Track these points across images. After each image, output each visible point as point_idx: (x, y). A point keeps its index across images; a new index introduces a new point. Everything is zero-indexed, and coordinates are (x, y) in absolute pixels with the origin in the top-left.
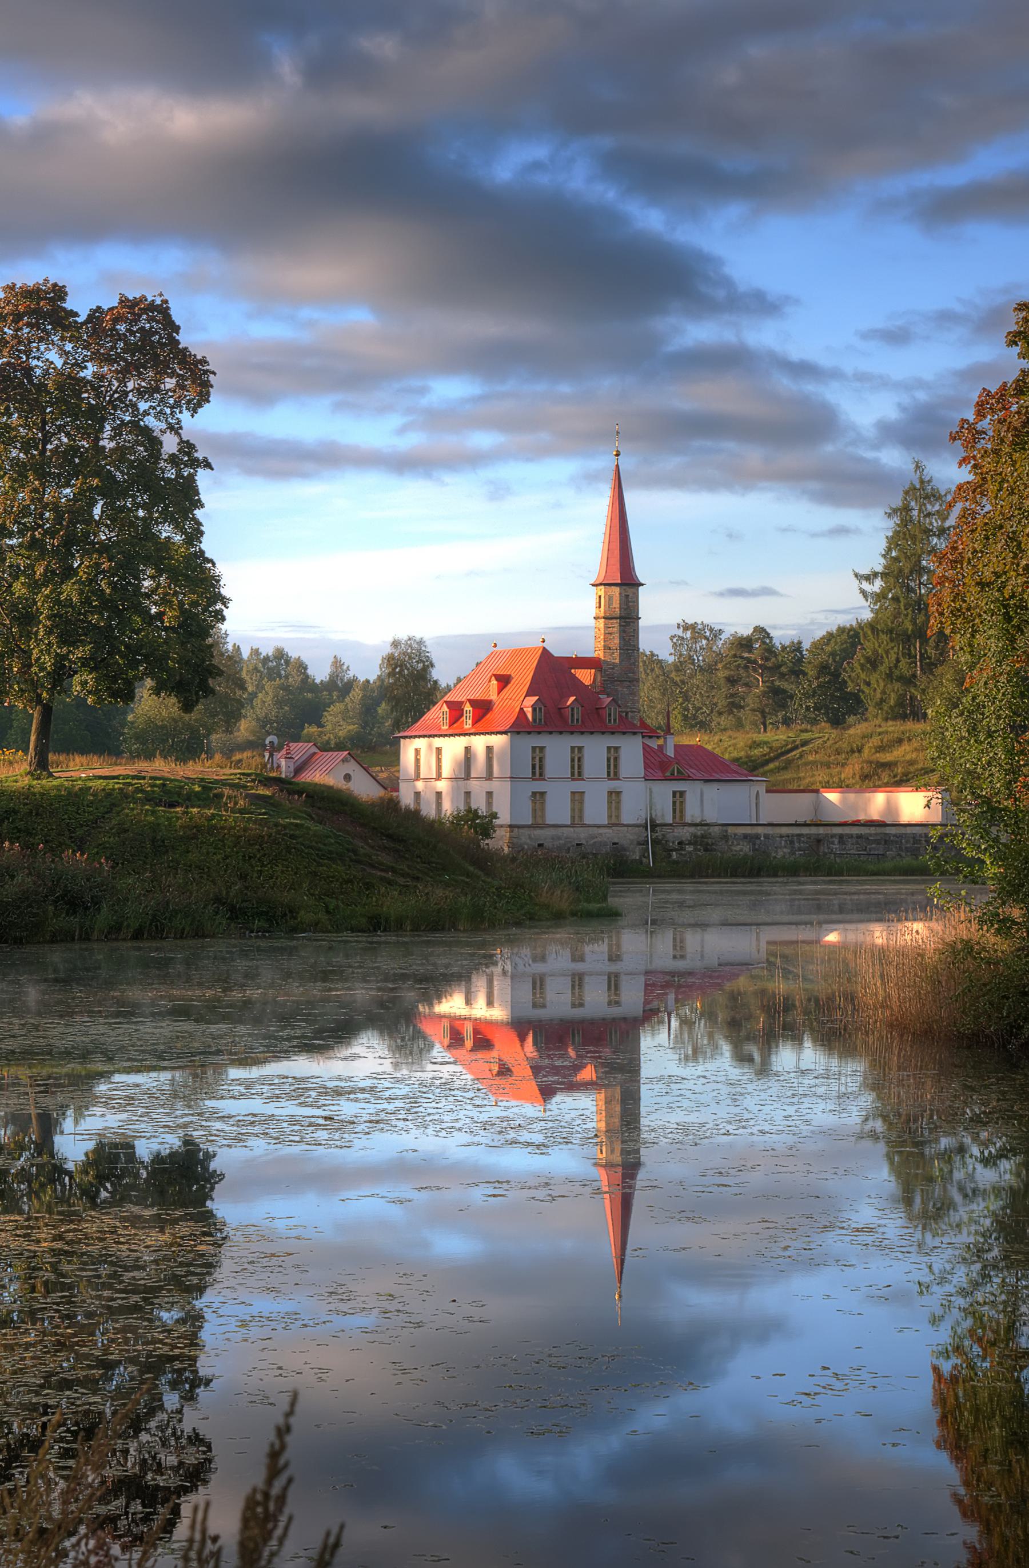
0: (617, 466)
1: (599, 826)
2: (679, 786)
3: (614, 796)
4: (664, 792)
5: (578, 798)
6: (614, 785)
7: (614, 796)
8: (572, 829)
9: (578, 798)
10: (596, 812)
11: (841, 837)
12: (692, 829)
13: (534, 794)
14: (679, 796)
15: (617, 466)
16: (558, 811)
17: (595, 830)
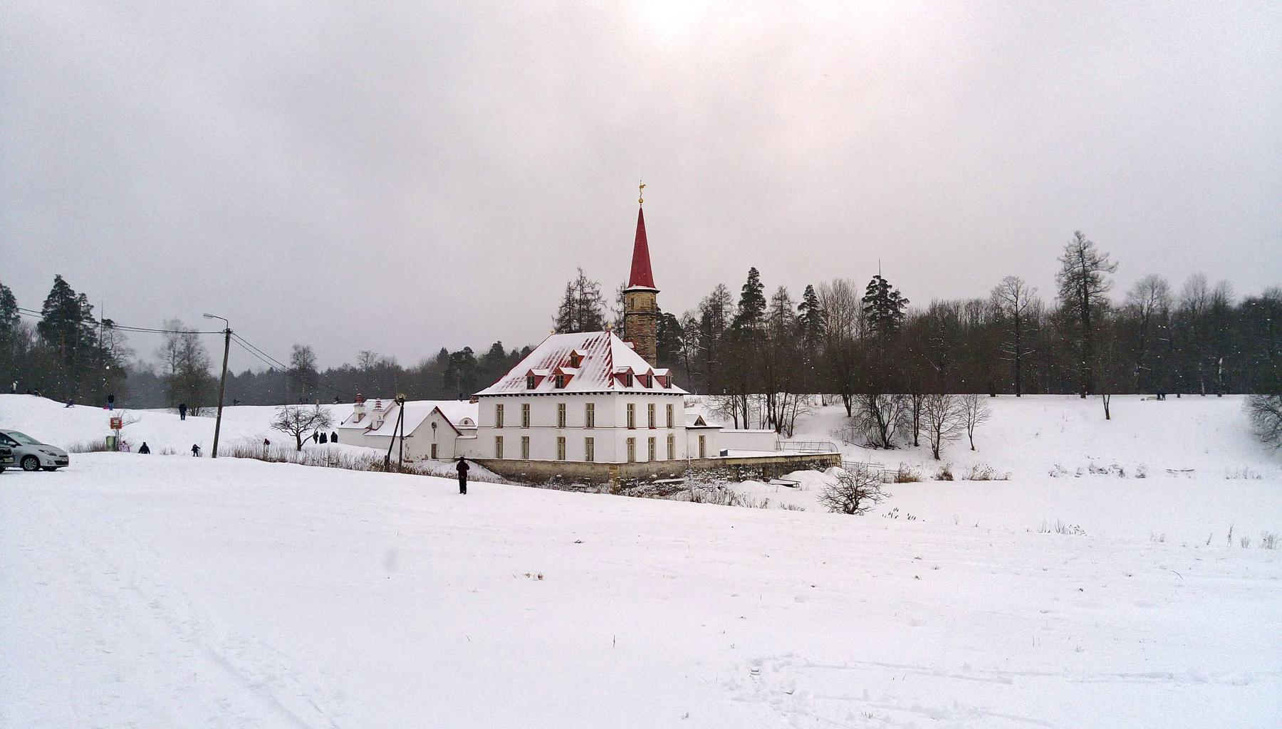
0: (641, 209)
1: (662, 462)
2: (703, 433)
3: (670, 439)
4: (694, 437)
5: (652, 440)
6: (671, 431)
7: (670, 439)
8: (647, 465)
9: (652, 440)
10: (661, 454)
11: (776, 463)
12: (709, 463)
13: (628, 439)
14: (702, 438)
15: (641, 209)
16: (642, 454)
17: (661, 466)
